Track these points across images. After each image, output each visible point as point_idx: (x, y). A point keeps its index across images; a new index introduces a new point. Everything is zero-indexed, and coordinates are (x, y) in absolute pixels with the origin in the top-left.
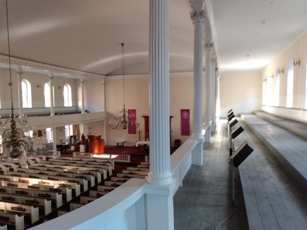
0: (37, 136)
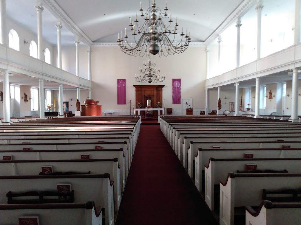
0: (24, 99)
